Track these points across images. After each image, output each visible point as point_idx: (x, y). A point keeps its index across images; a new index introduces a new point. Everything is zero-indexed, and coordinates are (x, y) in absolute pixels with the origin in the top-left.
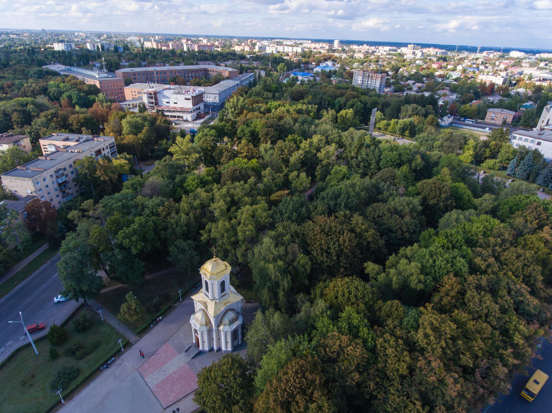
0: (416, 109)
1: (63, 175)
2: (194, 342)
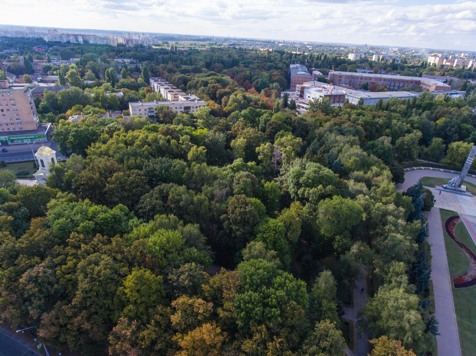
1: (153, 112)
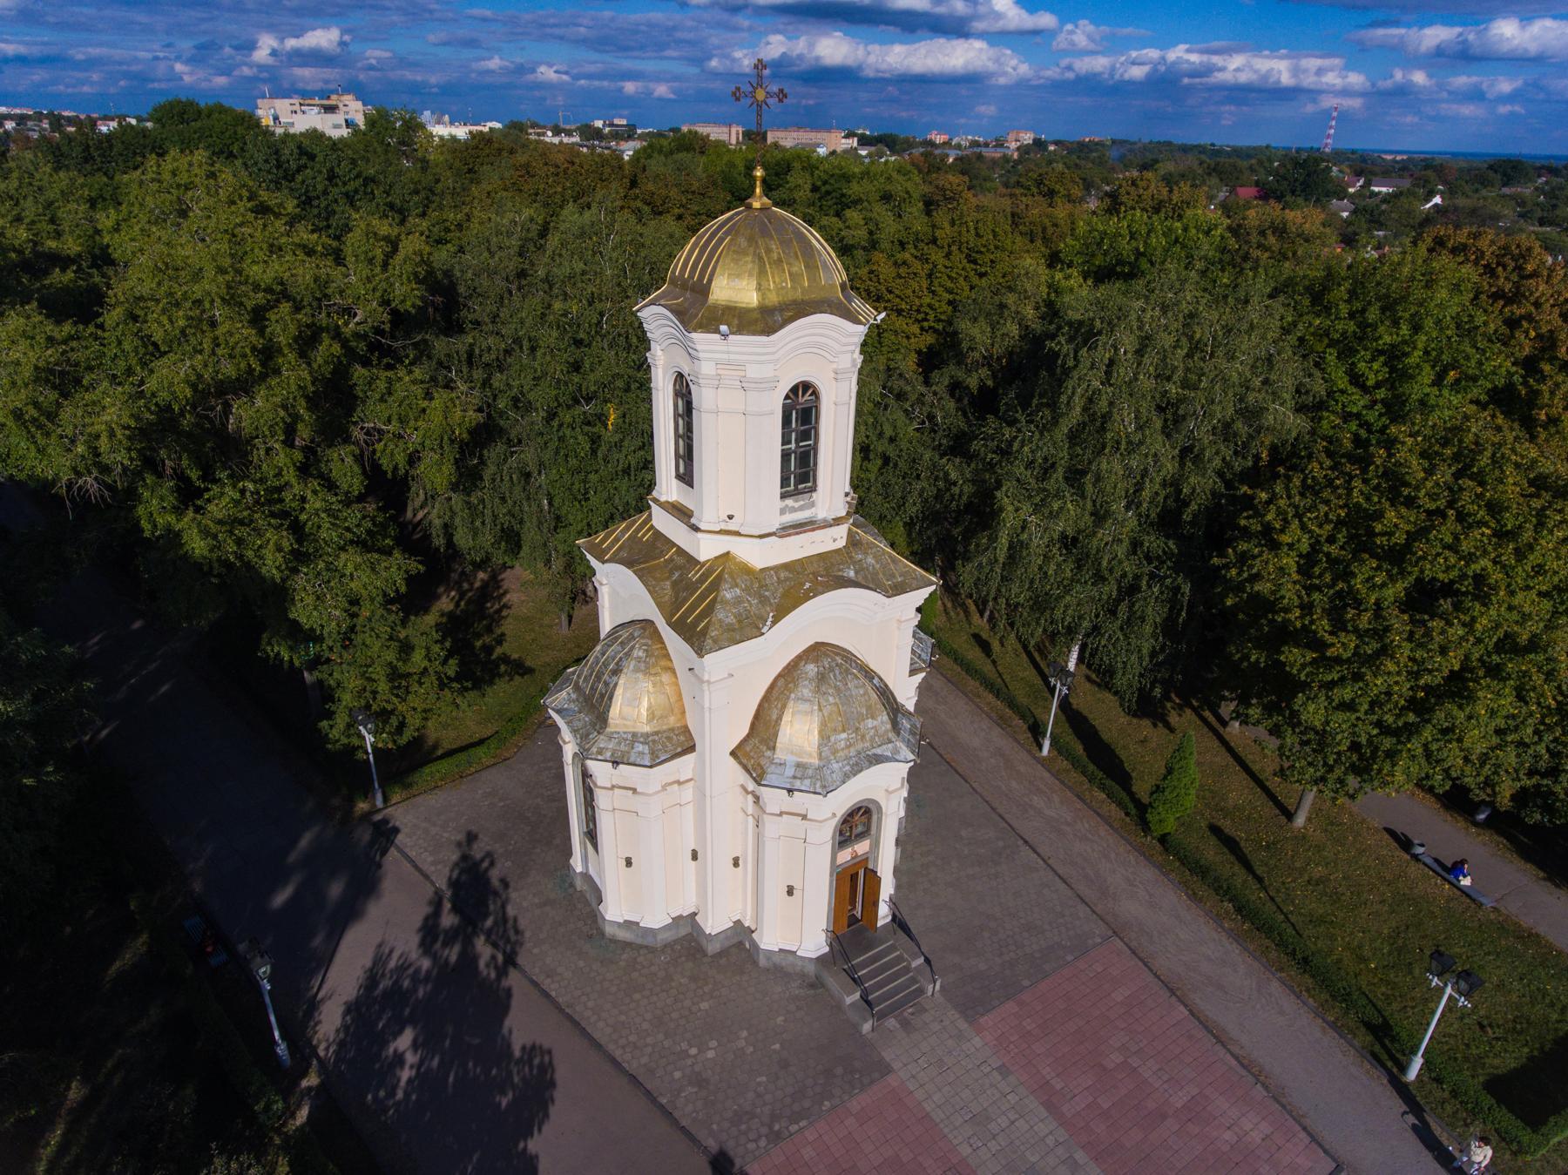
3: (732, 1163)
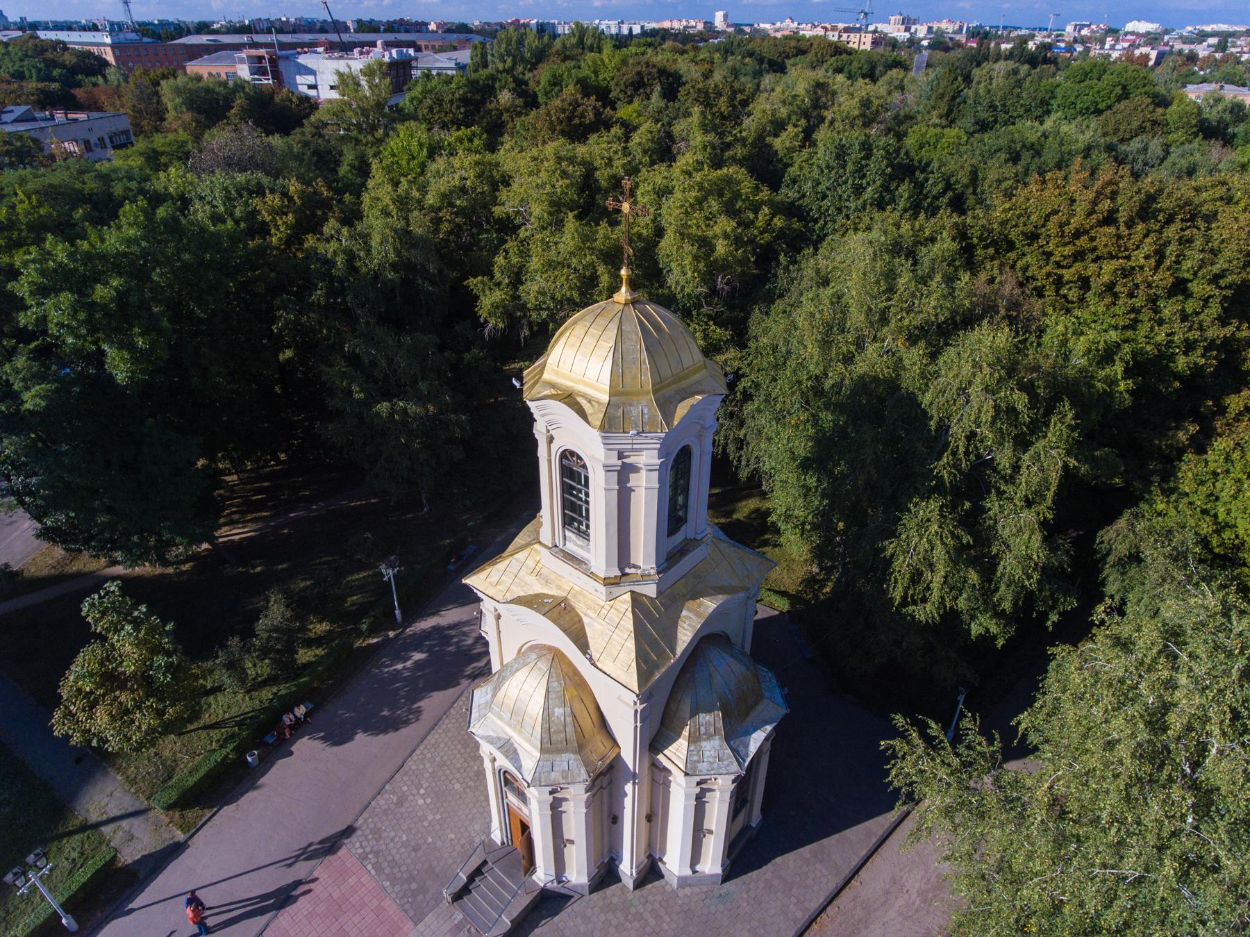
0: (1015, 72)
2: (497, 836)
3: (348, 837)
